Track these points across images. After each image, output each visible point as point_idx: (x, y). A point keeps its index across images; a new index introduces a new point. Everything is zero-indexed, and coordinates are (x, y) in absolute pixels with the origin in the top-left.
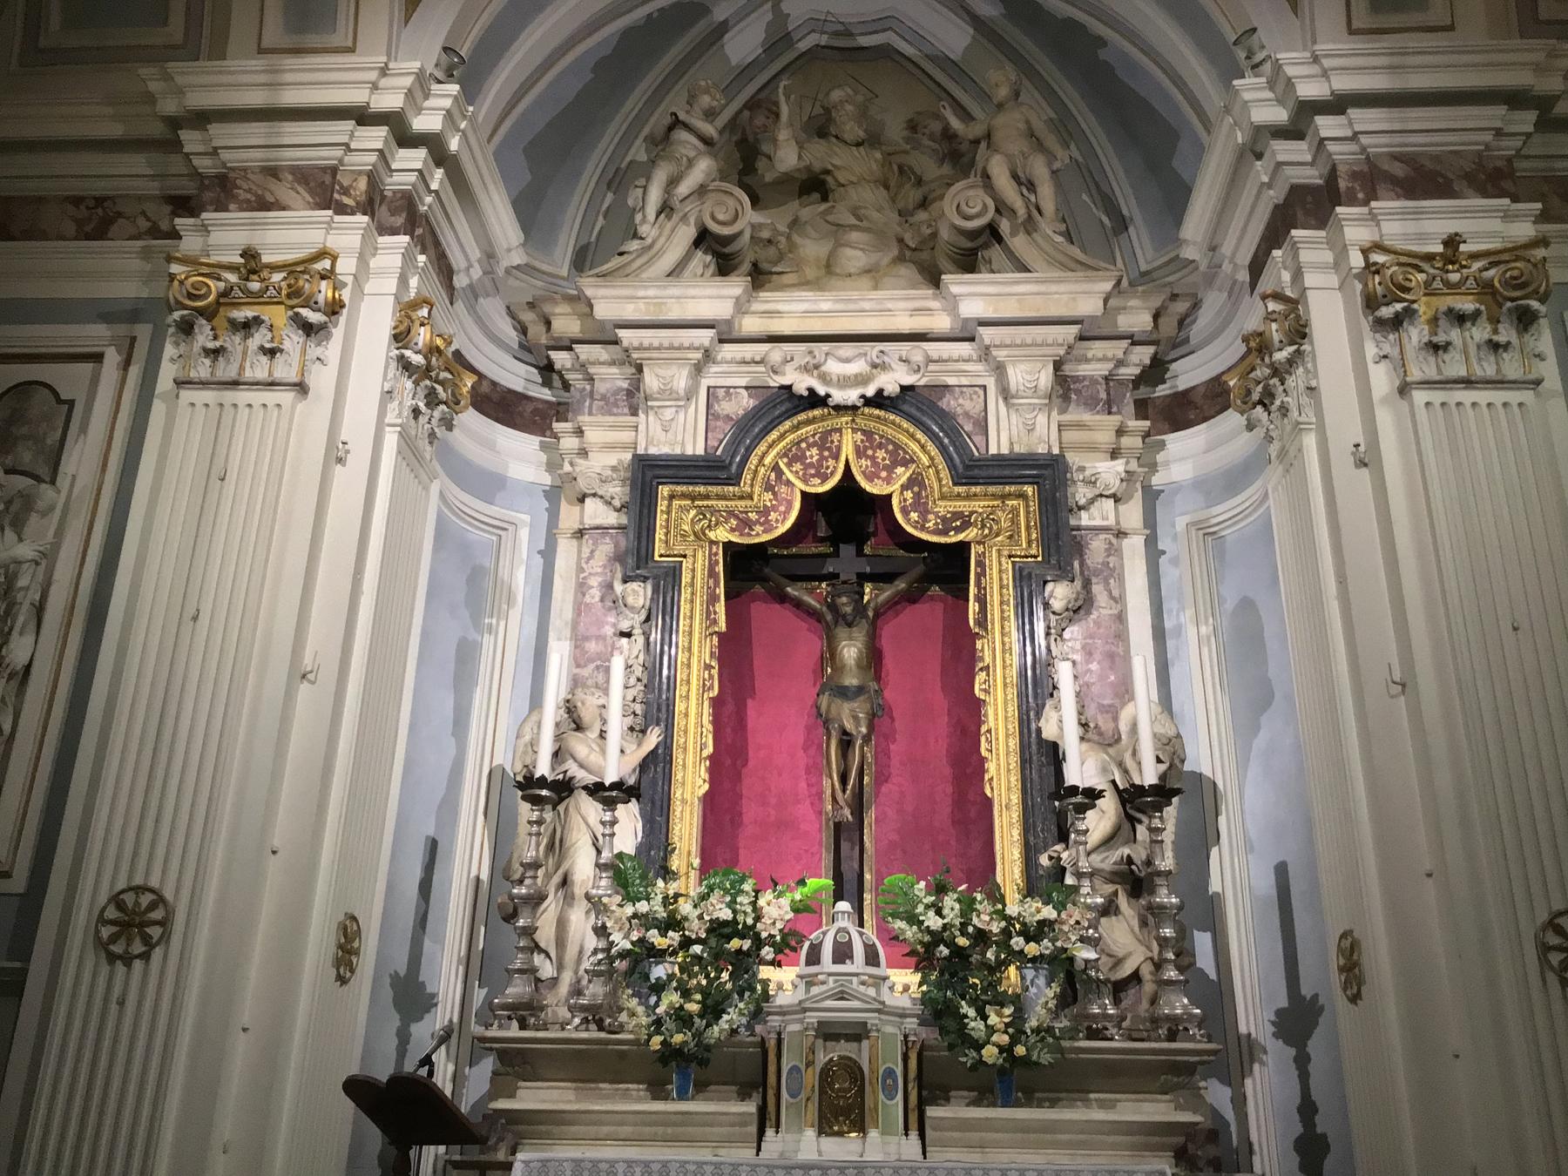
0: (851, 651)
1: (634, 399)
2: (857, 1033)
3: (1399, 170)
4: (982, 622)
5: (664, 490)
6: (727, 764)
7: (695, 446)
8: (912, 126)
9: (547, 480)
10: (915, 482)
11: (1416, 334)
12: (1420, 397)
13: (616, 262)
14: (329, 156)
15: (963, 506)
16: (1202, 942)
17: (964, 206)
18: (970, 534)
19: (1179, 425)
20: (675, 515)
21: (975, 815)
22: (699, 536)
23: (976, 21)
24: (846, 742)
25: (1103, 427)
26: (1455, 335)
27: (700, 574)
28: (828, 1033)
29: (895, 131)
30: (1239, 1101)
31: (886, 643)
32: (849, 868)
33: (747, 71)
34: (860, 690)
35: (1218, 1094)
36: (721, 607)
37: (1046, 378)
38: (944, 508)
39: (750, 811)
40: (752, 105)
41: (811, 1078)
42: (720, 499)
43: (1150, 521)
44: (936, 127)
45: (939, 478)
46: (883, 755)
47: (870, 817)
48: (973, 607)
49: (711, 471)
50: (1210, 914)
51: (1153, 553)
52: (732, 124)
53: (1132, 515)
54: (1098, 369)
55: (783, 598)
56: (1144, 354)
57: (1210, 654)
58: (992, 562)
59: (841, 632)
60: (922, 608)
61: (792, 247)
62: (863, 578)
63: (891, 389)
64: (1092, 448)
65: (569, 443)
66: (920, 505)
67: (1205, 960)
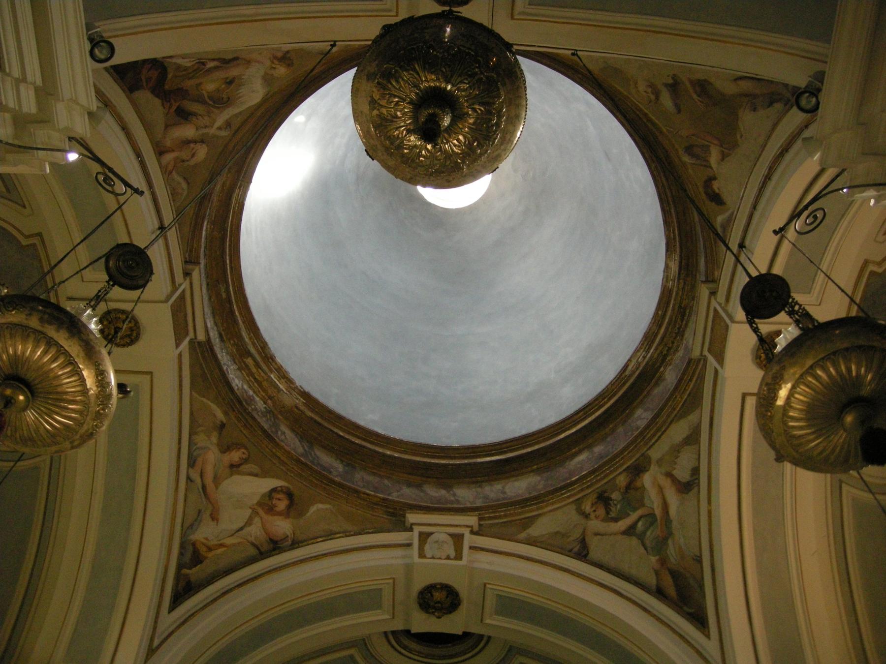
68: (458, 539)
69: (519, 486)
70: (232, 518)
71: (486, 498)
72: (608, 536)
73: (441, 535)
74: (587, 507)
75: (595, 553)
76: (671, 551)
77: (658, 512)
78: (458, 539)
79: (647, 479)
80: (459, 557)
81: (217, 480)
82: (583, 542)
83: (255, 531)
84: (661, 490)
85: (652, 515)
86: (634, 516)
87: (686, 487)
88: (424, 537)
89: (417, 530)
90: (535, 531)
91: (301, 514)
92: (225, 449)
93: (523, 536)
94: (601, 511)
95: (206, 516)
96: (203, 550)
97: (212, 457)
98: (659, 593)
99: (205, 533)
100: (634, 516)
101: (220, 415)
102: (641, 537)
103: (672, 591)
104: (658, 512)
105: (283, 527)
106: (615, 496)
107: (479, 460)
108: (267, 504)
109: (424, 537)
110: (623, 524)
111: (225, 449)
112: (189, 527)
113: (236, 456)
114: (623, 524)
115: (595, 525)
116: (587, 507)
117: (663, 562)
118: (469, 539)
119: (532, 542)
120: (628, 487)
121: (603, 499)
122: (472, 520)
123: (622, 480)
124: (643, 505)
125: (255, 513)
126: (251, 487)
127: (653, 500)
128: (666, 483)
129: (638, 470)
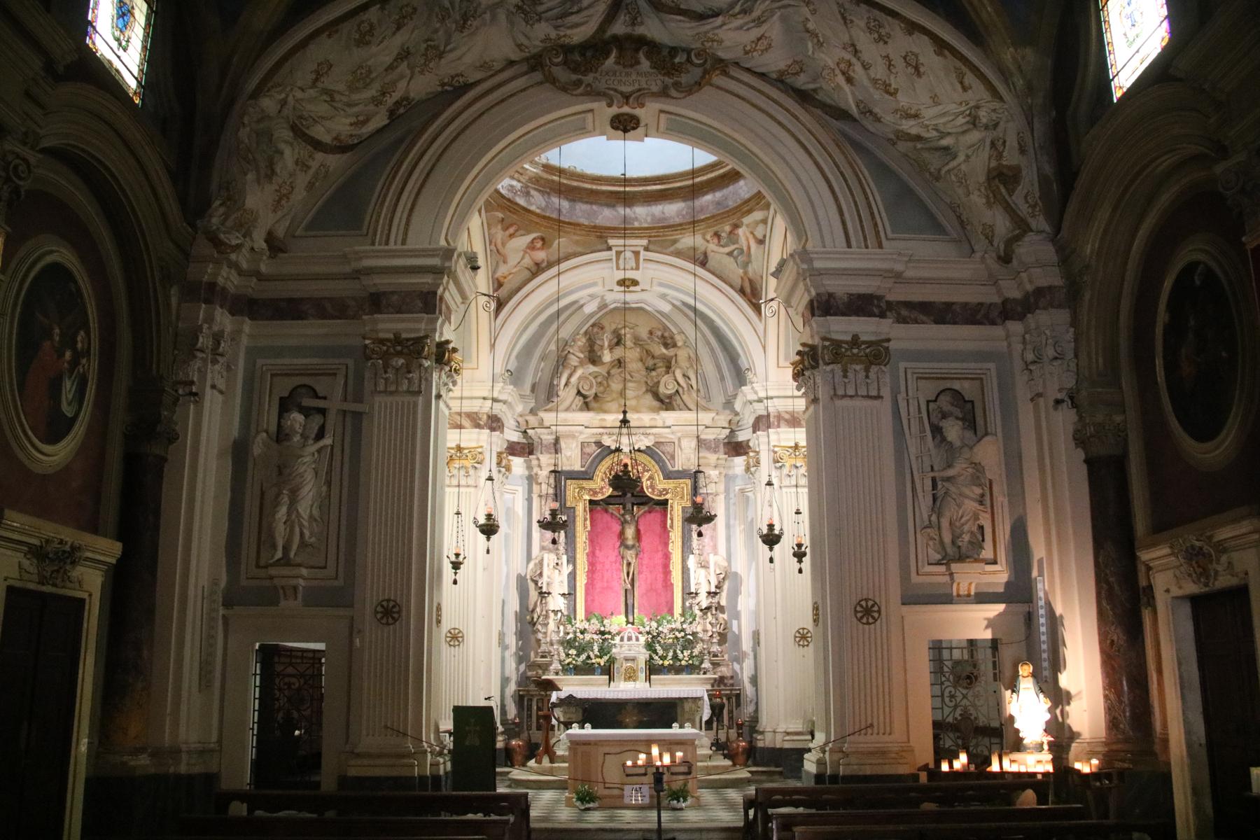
0: (630, 532)
1: (556, 446)
2: (633, 660)
3: (787, 416)
4: (672, 527)
5: (569, 482)
6: (592, 571)
7: (577, 467)
8: (651, 333)
9: (527, 473)
10: (651, 478)
11: (785, 471)
12: (784, 490)
13: (551, 405)
14: (475, 410)
15: (666, 486)
16: (735, 623)
17: (667, 387)
18: (668, 497)
19: (738, 454)
20: (571, 487)
21: (668, 586)
22: (581, 497)
23: (674, 305)
24: (629, 564)
25: (712, 458)
26: (794, 472)
27: (581, 510)
28: (627, 660)
29: (644, 334)
30: (742, 669)
31: (641, 528)
32: (630, 602)
33: (592, 315)
34: (633, 546)
35: (736, 666)
36: (588, 522)
37: (694, 443)
38: (660, 487)
39: (598, 585)
40: (593, 326)
41: (623, 670)
42: (585, 484)
43: (727, 491)
44: (659, 333)
45: (659, 476)
46: (641, 565)
47: (636, 585)
48: (669, 522)
49: (586, 476)
50: (737, 615)
51: (727, 498)
52: (586, 333)
53: (721, 487)
54: (712, 437)
55: (606, 511)
56: (728, 431)
57: (742, 536)
58: (675, 506)
59: (627, 526)
60: (652, 515)
61: (608, 386)
62: (633, 504)
63: (643, 448)
64: (708, 465)
65: (535, 462)
66: (652, 487)
67: (735, 629)
68: (637, 254)
69: (672, 210)
70: (513, 259)
71: (653, 215)
72: (718, 254)
73: (629, 254)
74: (708, 237)
75: (710, 264)
76: (750, 269)
77: (745, 249)
78: (637, 254)
79: (740, 231)
80: (637, 268)
81: (503, 244)
82: (705, 254)
83: (527, 261)
84: (747, 239)
85: (742, 250)
86: (732, 247)
87: (761, 242)
88: (618, 254)
89: (614, 249)
90: (679, 246)
91: (550, 246)
92: (505, 229)
93: (672, 249)
94: (716, 241)
95: (501, 263)
96: (502, 280)
97: (500, 235)
98: (742, 291)
99: (502, 270)
100: (732, 247)
101: (500, 215)
102: (736, 258)
103: (748, 290)
104: (745, 249)
105: (541, 255)
106: (723, 234)
107: (649, 188)
108: (531, 246)
109: (618, 254)
110: (727, 250)
111: (505, 229)
112: (494, 272)
113: (511, 230)
114: (727, 250)
115: (712, 246)
116: (708, 237)
117: (746, 273)
118: (643, 254)
119: (678, 254)
120: (731, 232)
121: (717, 235)
122: (644, 242)
123: (728, 228)
124: (736, 242)
125: (525, 252)
126: (523, 241)
127: (743, 240)
128: (751, 237)
129: (736, 226)
